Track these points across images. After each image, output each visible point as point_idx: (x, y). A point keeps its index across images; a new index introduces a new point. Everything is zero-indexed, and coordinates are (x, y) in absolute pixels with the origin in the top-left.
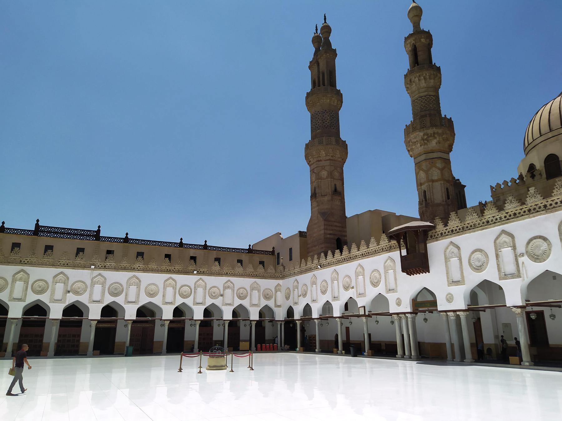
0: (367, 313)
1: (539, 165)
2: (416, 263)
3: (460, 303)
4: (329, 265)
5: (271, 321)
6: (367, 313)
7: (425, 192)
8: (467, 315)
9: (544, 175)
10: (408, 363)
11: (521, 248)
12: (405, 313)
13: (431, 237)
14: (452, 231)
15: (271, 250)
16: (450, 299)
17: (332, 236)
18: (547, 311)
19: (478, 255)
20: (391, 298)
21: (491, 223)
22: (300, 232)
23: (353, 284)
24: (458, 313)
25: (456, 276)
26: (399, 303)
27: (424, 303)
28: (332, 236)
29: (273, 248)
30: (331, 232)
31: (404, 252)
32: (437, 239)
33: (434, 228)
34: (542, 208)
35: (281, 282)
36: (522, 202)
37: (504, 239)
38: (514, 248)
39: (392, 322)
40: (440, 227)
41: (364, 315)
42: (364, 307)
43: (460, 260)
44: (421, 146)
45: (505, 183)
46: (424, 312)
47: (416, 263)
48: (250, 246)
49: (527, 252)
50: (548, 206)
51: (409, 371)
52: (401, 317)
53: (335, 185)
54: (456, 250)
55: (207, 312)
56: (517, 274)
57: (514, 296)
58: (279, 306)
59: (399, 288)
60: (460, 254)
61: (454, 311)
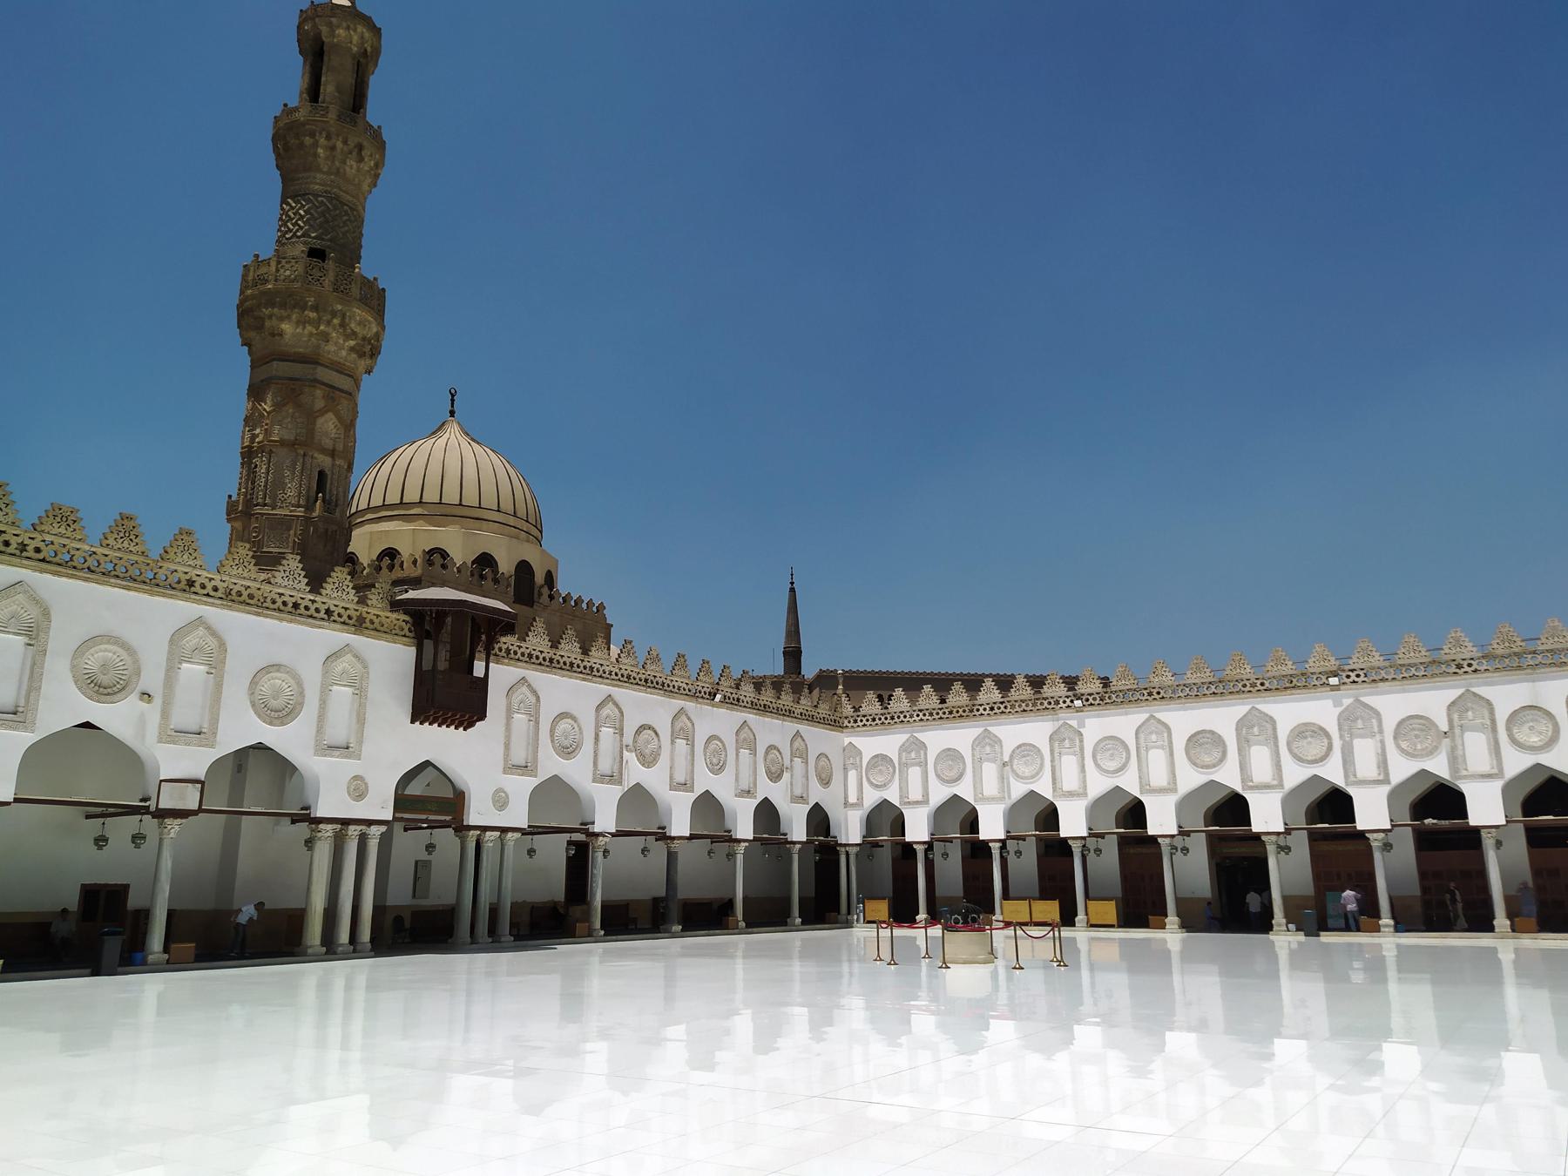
2: (448, 696)
10: (340, 969)
11: (628, 738)
12: (370, 823)
14: (530, 656)
19: (564, 725)
21: (234, 597)
23: (152, 678)
26: (358, 789)
27: (430, 802)
34: (183, 585)
36: (316, 582)
39: (310, 843)
43: (537, 722)
44: (352, 349)
46: (433, 826)
47: (448, 696)
50: (197, 584)
51: (360, 996)
54: (533, 700)
59: (367, 749)
60: (537, 712)
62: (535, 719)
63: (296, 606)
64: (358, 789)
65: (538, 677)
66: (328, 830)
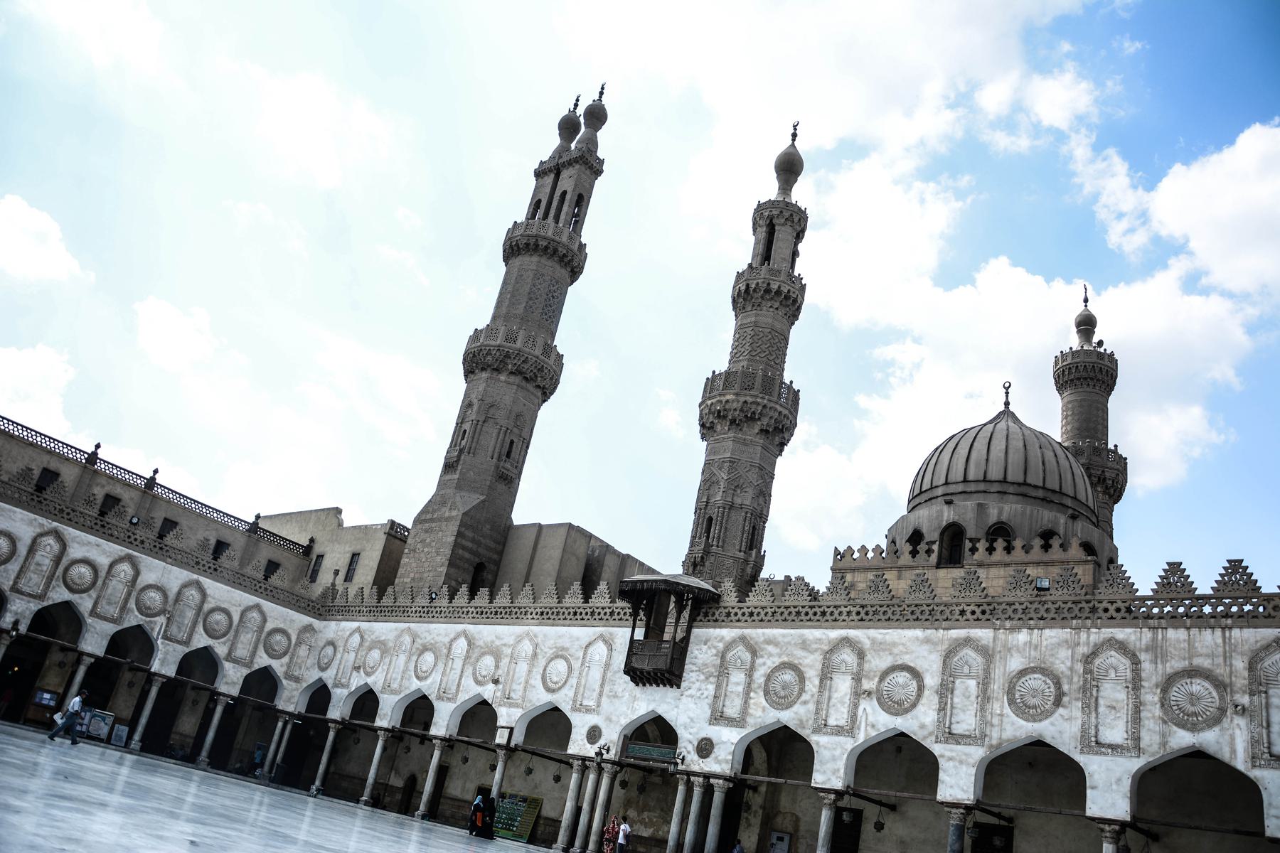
0: (512, 744)
1: (931, 534)
3: (722, 763)
4: (454, 616)
5: (260, 708)
6: (512, 744)
7: (710, 519)
8: (729, 788)
9: (934, 557)
13: (706, 615)
15: (305, 542)
16: (705, 748)
17: (467, 555)
18: (871, 812)
19: (788, 676)
20: (580, 724)
22: (393, 523)
24: (712, 781)
25: (732, 710)
26: (594, 734)
28: (467, 555)
29: (312, 540)
30: (469, 545)
31: (640, 634)
32: (716, 623)
33: (715, 599)
35: (316, 623)
37: (844, 656)
38: (857, 679)
40: (730, 599)
41: (507, 747)
42: (512, 729)
45: (864, 549)
48: (258, 517)
49: (878, 690)
52: (587, 768)
53: (512, 442)
54: (747, 656)
55: (118, 643)
56: (849, 730)
57: (831, 768)
58: (297, 680)
61: (707, 776)
62: (750, 673)
63: (575, 614)
64: (594, 734)
65: (757, 634)
66: (576, 763)
